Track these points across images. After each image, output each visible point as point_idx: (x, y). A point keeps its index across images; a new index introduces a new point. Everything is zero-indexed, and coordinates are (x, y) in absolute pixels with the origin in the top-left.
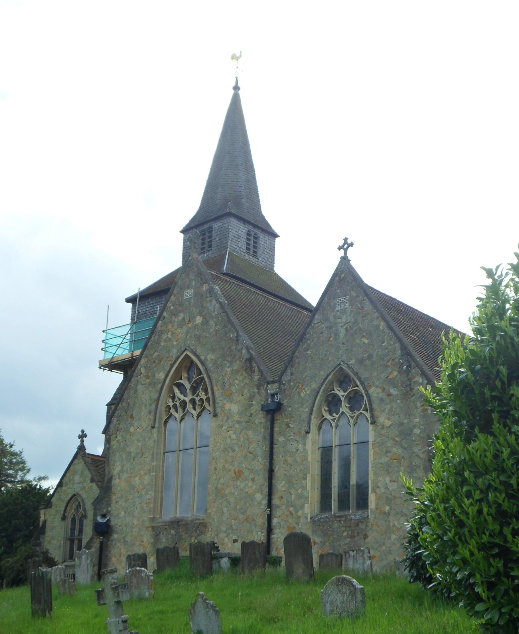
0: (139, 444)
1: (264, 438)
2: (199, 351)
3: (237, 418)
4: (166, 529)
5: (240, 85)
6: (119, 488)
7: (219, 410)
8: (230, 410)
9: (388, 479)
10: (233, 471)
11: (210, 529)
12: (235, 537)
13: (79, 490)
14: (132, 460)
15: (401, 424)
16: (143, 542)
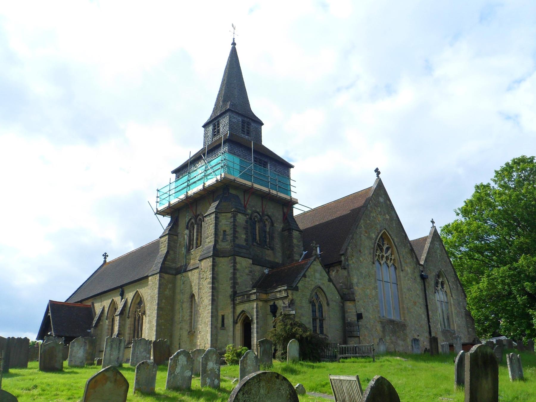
0: (367, 270)
1: (421, 289)
2: (390, 233)
3: (410, 275)
4: (388, 324)
5: (235, 42)
6: (358, 293)
7: (403, 269)
8: (407, 270)
9: (458, 319)
10: (412, 301)
11: (408, 328)
12: (418, 334)
13: (320, 284)
14: (364, 278)
15: (458, 300)
16: (377, 329)
